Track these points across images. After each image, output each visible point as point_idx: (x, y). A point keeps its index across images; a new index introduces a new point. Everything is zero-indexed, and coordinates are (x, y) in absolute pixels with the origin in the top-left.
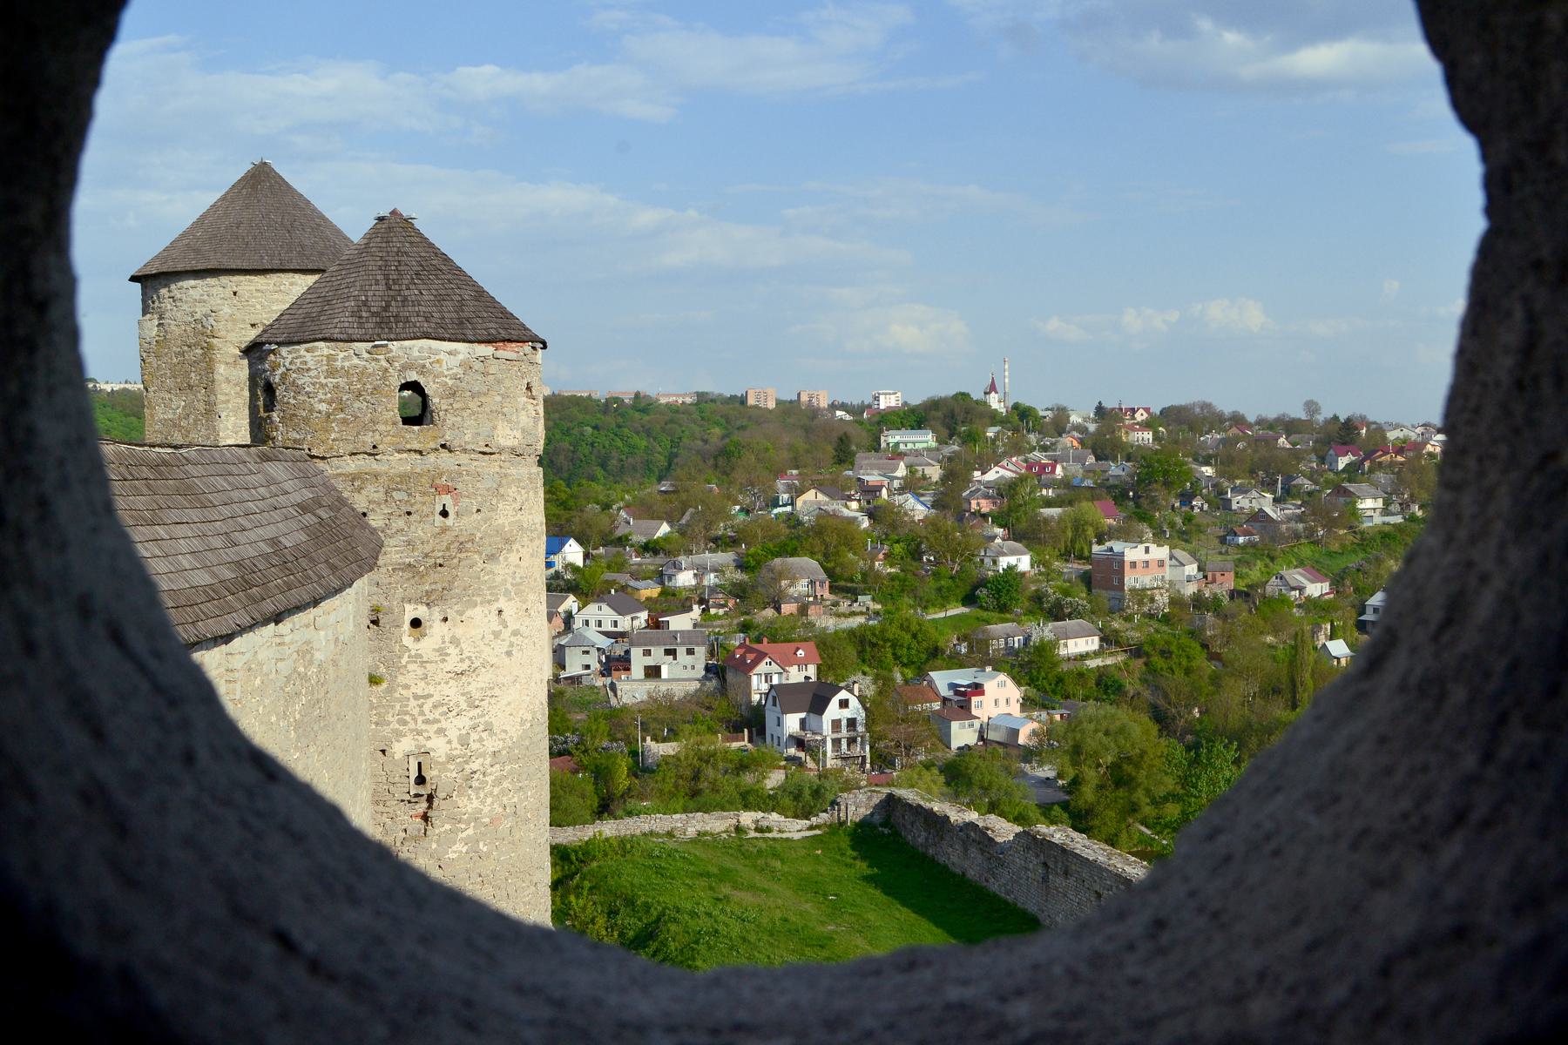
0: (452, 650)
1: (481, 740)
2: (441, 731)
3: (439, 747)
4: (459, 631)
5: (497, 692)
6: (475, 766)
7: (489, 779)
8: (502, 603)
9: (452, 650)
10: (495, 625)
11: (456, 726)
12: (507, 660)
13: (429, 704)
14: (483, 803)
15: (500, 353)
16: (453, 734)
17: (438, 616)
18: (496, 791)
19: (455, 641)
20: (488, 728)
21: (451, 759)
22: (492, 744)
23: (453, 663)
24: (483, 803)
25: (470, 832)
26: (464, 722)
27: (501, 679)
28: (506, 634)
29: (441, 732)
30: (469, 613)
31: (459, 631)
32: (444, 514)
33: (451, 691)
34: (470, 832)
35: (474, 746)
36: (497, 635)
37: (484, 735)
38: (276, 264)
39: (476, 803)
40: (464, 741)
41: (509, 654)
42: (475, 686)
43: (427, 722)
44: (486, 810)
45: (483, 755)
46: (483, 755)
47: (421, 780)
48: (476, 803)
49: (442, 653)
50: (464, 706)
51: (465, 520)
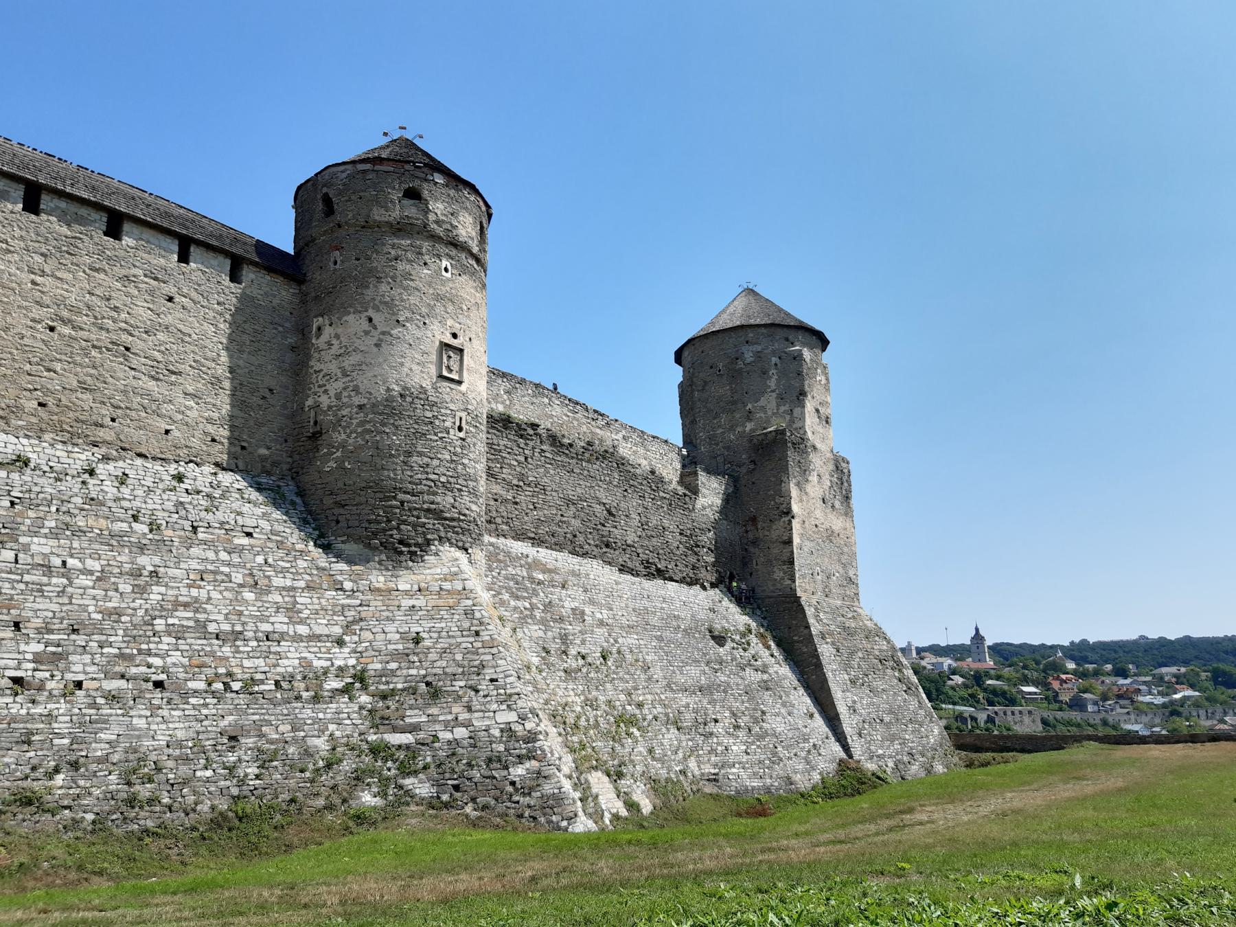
0: (334, 342)
1: (350, 396)
2: (326, 392)
3: (325, 401)
4: (340, 330)
5: (364, 367)
6: (344, 413)
7: (355, 422)
8: (371, 313)
9: (334, 342)
10: (365, 325)
11: (334, 387)
12: (375, 349)
13: (321, 375)
14: (349, 437)
15: (377, 167)
16: (332, 393)
17: (327, 322)
18: (359, 430)
19: (337, 337)
20: (356, 389)
21: (330, 407)
22: (357, 400)
23: (335, 350)
24: (349, 437)
25: (339, 454)
26: (339, 385)
27: (368, 360)
28: (374, 333)
29: (326, 392)
30: (345, 318)
31: (340, 330)
32: (335, 263)
33: (333, 367)
34: (339, 454)
35: (345, 400)
36: (367, 333)
37: (353, 394)
38: (720, 335)
39: (344, 436)
40: (338, 396)
41: (377, 345)
42: (348, 362)
43: (320, 386)
44: (351, 441)
45: (351, 406)
46: (351, 406)
47: (316, 423)
48: (344, 436)
49: (330, 344)
50: (339, 375)
51: (347, 264)
